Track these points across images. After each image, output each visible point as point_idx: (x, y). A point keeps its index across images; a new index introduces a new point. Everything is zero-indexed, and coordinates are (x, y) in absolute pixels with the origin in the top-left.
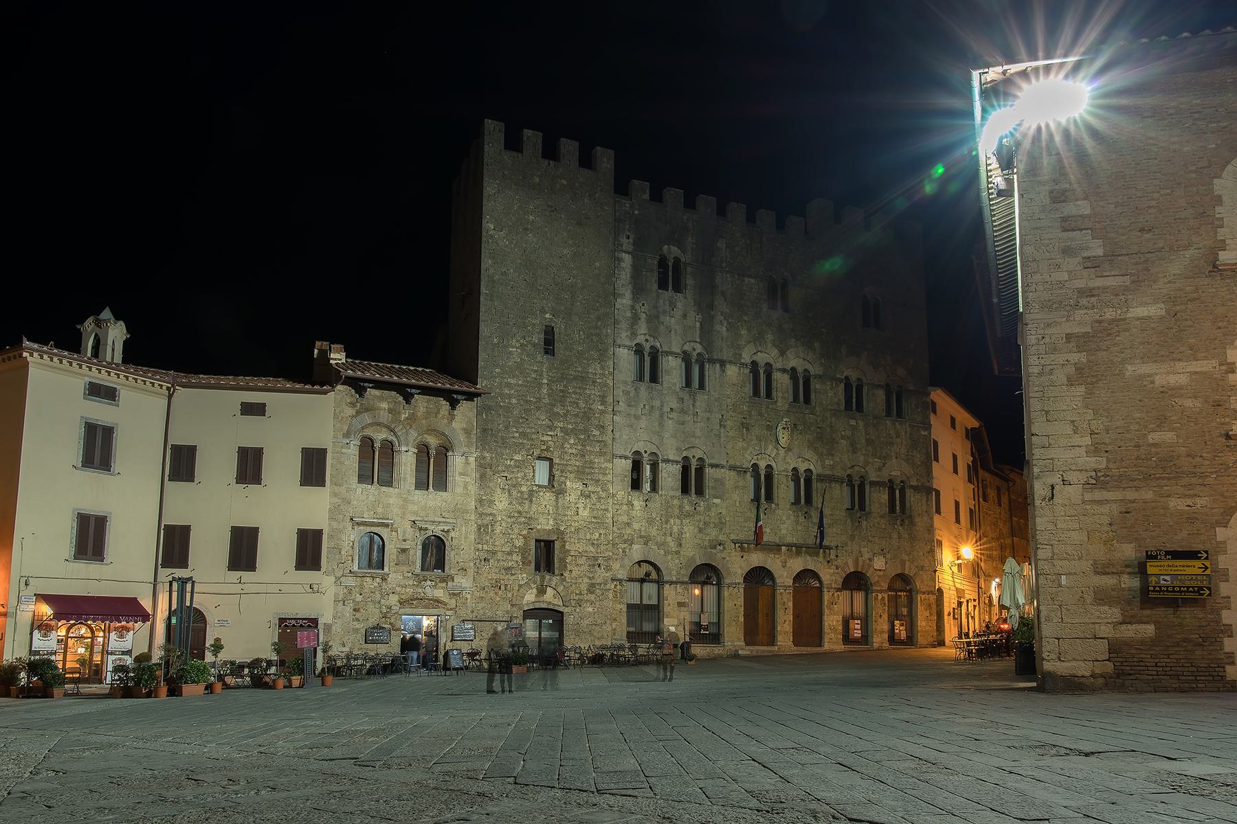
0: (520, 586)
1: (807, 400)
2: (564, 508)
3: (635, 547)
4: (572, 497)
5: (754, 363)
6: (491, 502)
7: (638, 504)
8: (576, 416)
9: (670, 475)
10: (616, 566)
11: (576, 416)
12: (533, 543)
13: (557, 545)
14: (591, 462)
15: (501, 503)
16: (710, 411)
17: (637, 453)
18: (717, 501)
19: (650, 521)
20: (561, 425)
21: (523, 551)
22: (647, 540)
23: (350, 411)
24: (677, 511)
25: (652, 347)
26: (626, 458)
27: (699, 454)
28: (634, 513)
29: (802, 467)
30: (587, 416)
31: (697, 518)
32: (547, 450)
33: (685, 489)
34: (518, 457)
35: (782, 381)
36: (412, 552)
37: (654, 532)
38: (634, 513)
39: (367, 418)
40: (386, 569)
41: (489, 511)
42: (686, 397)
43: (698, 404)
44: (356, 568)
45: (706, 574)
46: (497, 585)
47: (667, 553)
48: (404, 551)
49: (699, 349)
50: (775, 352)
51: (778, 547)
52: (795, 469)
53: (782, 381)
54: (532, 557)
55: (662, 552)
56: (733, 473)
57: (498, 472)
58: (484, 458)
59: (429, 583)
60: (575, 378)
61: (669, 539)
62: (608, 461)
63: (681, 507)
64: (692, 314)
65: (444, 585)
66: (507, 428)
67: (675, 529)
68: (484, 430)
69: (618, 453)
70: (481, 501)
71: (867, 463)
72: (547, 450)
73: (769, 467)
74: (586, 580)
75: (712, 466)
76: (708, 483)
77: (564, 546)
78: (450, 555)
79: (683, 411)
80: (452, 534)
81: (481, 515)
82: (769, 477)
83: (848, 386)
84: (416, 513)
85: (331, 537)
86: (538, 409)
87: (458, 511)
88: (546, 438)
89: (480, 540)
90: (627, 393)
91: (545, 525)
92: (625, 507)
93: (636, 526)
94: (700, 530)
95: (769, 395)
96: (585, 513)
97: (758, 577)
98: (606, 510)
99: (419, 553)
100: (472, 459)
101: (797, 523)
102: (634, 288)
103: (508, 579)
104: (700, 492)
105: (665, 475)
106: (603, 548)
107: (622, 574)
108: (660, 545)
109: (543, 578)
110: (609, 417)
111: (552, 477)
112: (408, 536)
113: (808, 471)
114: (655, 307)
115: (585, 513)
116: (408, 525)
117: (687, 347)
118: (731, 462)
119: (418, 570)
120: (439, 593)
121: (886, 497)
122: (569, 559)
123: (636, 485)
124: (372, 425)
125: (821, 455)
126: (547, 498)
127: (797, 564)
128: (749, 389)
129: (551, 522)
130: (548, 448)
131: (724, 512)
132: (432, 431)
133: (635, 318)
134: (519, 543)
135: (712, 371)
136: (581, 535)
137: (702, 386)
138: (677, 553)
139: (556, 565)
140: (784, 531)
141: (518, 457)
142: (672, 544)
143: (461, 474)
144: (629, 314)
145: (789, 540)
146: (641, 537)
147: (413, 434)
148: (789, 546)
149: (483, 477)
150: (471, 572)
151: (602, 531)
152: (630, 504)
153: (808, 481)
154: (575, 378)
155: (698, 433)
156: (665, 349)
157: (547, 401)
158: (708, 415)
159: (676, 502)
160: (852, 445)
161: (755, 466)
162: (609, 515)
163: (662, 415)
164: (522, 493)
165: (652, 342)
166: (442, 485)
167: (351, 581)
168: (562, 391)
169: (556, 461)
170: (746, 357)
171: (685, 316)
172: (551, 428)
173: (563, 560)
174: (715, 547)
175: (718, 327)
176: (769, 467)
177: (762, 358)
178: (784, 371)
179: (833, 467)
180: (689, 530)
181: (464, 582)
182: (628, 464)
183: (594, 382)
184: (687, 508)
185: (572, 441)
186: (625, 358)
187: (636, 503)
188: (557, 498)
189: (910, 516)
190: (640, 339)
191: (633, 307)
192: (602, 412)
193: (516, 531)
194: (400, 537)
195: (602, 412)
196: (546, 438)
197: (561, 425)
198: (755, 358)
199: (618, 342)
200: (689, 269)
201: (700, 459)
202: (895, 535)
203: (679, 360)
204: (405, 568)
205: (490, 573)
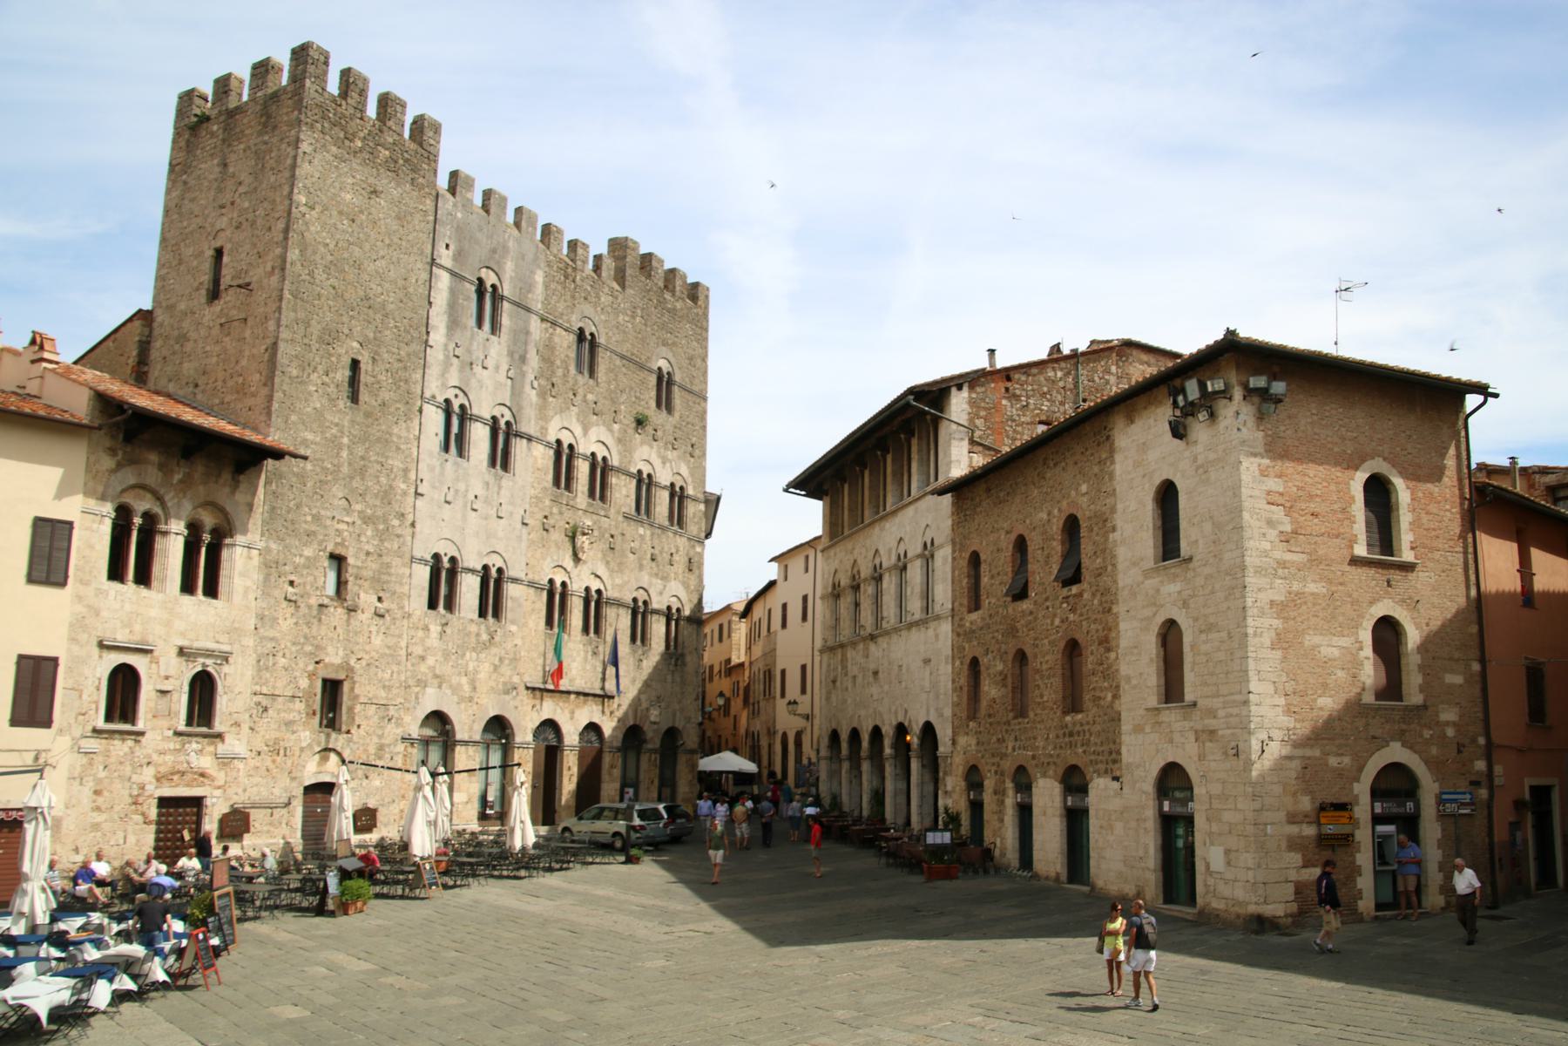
0: (302, 749)
1: (603, 498)
2: (356, 633)
3: (430, 691)
4: (364, 617)
5: (559, 442)
6: (275, 619)
7: (435, 629)
8: (376, 496)
9: (469, 588)
10: (407, 719)
11: (376, 496)
12: (319, 684)
13: (346, 687)
14: (388, 566)
15: (286, 622)
16: (512, 503)
17: (436, 557)
18: (514, 628)
19: (446, 655)
20: (358, 507)
21: (309, 694)
22: (440, 680)
23: (108, 462)
24: (473, 640)
25: (462, 407)
26: (426, 562)
27: (500, 563)
28: (429, 643)
29: (595, 585)
30: (387, 496)
31: (494, 650)
32: (342, 544)
33: (482, 613)
34: (308, 552)
35: (582, 469)
36: (175, 696)
37: (446, 669)
38: (429, 643)
39: (129, 477)
40: (140, 726)
41: (271, 633)
42: (492, 481)
43: (503, 492)
44: (100, 723)
45: (499, 727)
46: (276, 749)
47: (462, 700)
48: (163, 692)
49: (508, 417)
50: (578, 430)
51: (569, 693)
52: (587, 589)
53: (582, 469)
54: (317, 707)
55: (455, 699)
56: (532, 591)
57: (285, 574)
58: (268, 550)
59: (195, 746)
60: (378, 440)
61: (464, 680)
62: (404, 565)
63: (478, 635)
64: (505, 367)
65: (211, 749)
66: (298, 506)
67: (471, 668)
68: (273, 509)
69: (418, 554)
70: (262, 618)
71: (650, 584)
72: (342, 544)
73: (564, 584)
74: (375, 740)
75: (515, 580)
76: (508, 604)
77: (352, 689)
78: (222, 703)
79: (487, 501)
80: (226, 669)
81: (262, 638)
82: (564, 596)
83: (640, 481)
84: (183, 634)
85: (69, 669)
86: (336, 480)
87: (234, 632)
88: (343, 526)
89: (258, 678)
90: (432, 469)
91: (334, 657)
92: (420, 633)
93: (431, 661)
94: (496, 668)
95: (568, 487)
96: (377, 641)
97: (550, 725)
98: (400, 636)
99: (185, 698)
100: (255, 552)
101: (586, 659)
102: (450, 315)
103: (290, 740)
104: (496, 615)
105: (464, 589)
106: (395, 691)
107: (415, 731)
108: (455, 689)
109: (328, 736)
110: (410, 499)
111: (341, 584)
112: (172, 672)
113: (599, 592)
114: (469, 351)
115: (377, 641)
116: (174, 651)
117: (497, 412)
118: (530, 577)
119: (182, 727)
120: (206, 762)
121: (663, 629)
122: (358, 708)
123: (432, 605)
124: (133, 487)
125: (612, 571)
126: (337, 614)
127: (589, 713)
128: (550, 476)
129: (341, 653)
130: (344, 540)
131: (519, 642)
132: (211, 505)
133: (447, 365)
134: (304, 683)
135: (519, 446)
136: (373, 669)
137: (505, 466)
138: (471, 699)
139: (344, 717)
140: (574, 672)
141: (308, 552)
142: (467, 688)
143: (242, 575)
144: (441, 357)
145: (580, 685)
146: (436, 676)
147: (187, 507)
148: (578, 694)
149: (267, 577)
150: (245, 728)
151: (395, 668)
152: (426, 629)
153: (598, 603)
154: (378, 440)
155: (501, 534)
156: (475, 411)
157: (345, 469)
158: (510, 508)
159: (473, 628)
160: (640, 559)
161: (551, 581)
162: (403, 644)
163: (465, 506)
164: (310, 607)
165: (462, 400)
166: (212, 590)
167: (93, 744)
168: (363, 458)
169: (351, 561)
170: (552, 438)
171: (497, 368)
172: (348, 511)
173: (351, 709)
174: (507, 692)
175: (528, 388)
176: (564, 584)
177: (567, 439)
178: (585, 457)
179: (621, 587)
180: (485, 670)
181: (234, 744)
182: (423, 574)
183: (398, 448)
184: (485, 637)
185: (369, 533)
186: (434, 419)
187: (432, 627)
188: (348, 620)
189: (682, 655)
190: (450, 394)
191: (446, 345)
192: (405, 493)
193: (301, 665)
194: (163, 673)
195: (405, 493)
196: (343, 526)
197: (358, 507)
198: (560, 436)
199: (427, 394)
200: (506, 305)
201: (500, 571)
202: (669, 678)
203: (488, 429)
204: (164, 723)
205: (269, 729)
